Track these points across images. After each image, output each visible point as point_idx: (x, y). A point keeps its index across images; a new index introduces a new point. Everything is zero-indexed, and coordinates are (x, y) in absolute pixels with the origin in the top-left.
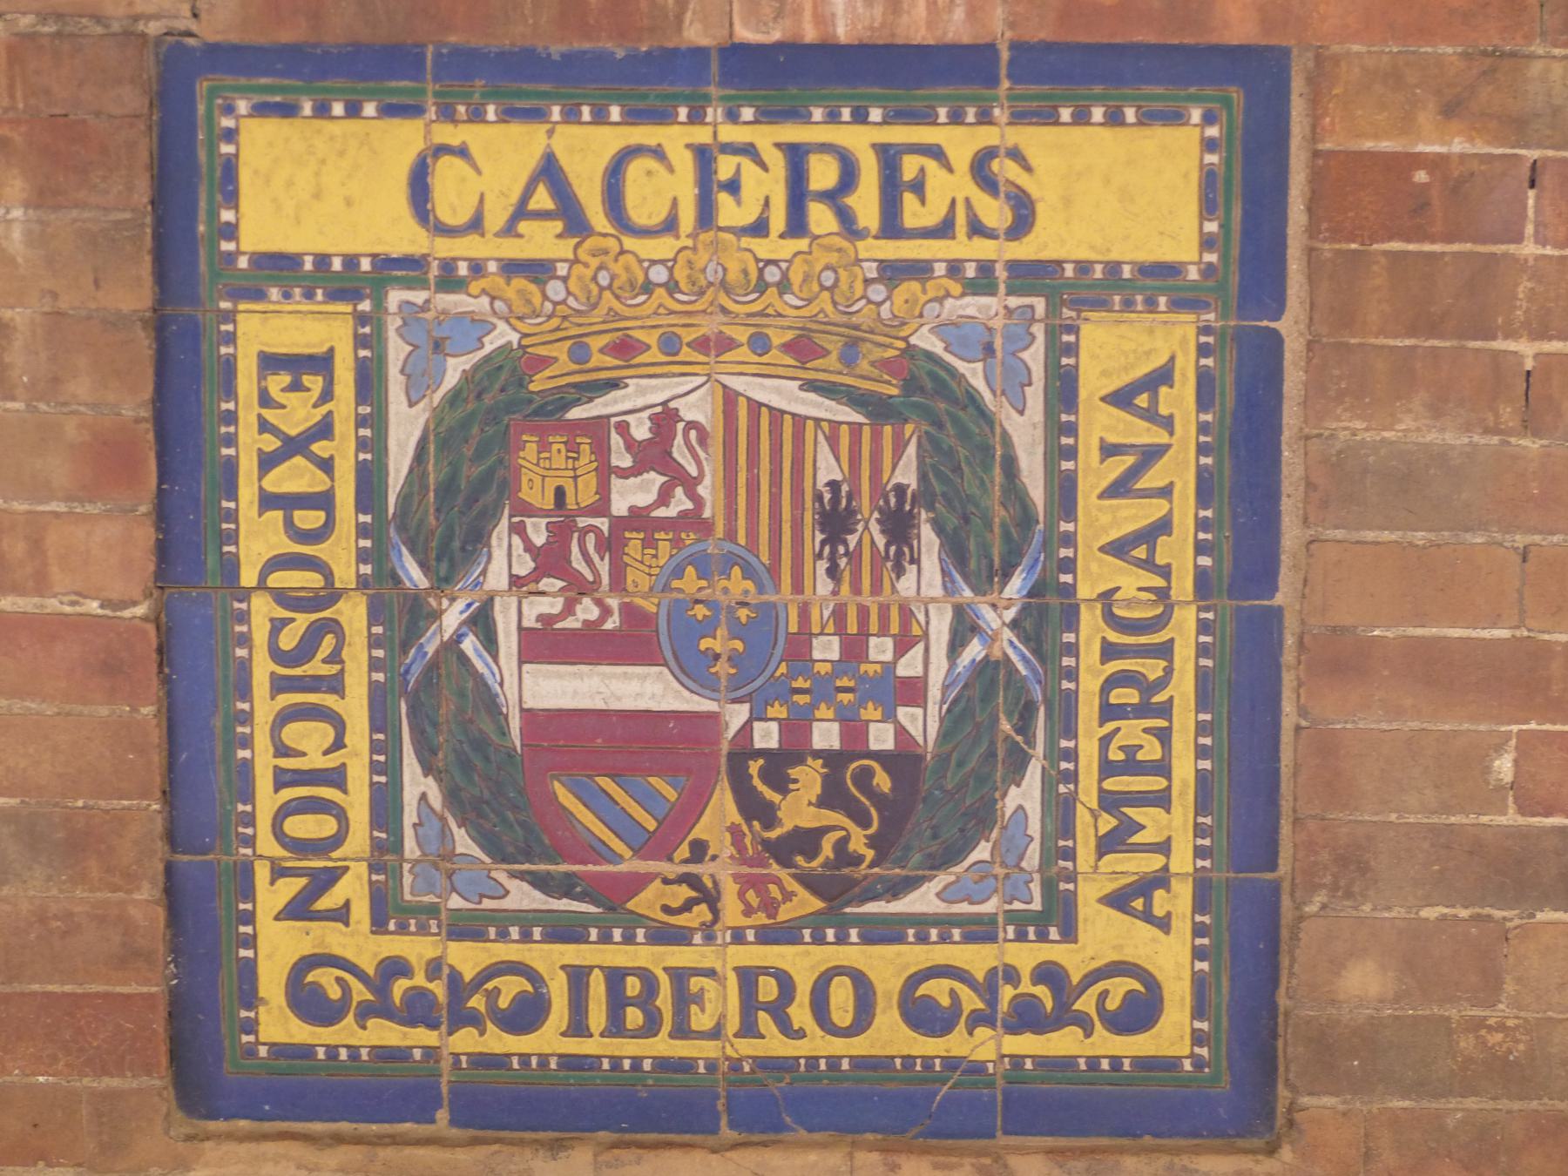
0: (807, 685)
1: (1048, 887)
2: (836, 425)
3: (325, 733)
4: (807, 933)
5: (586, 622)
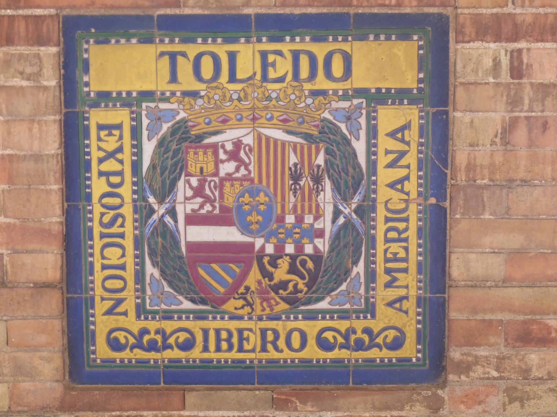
0: (283, 231)
1: (367, 300)
2: (295, 144)
3: (119, 251)
4: (284, 316)
5: (208, 211)
